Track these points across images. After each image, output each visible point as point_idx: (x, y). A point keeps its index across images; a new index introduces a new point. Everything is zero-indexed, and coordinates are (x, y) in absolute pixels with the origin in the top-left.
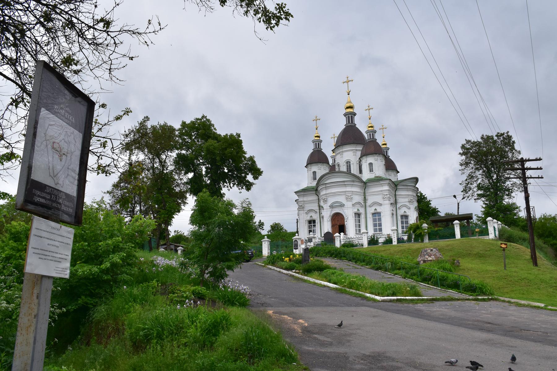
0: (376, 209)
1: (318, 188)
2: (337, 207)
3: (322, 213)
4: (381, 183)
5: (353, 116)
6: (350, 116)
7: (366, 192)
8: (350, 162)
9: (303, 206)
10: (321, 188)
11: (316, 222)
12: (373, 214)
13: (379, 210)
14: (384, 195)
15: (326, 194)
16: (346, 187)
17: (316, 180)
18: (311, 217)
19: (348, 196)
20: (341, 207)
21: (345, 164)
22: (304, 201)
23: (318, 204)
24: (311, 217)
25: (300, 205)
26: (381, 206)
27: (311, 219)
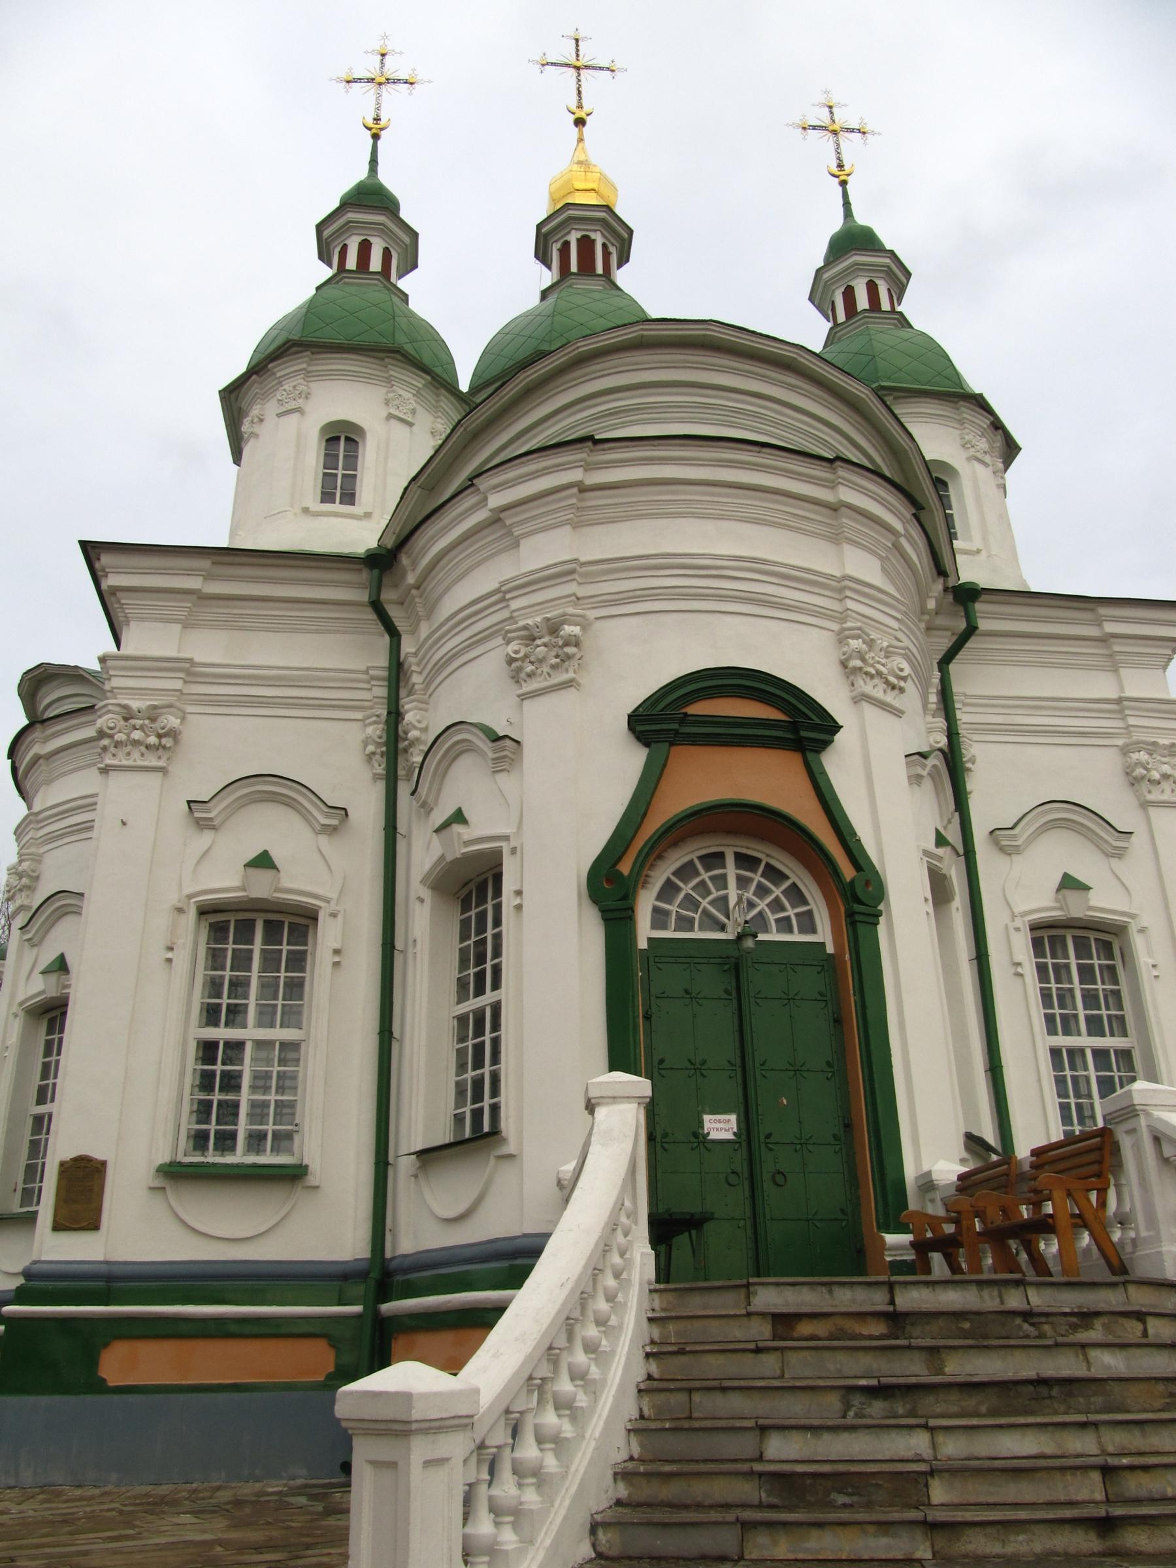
1: (430, 529)
3: (459, 817)
4: (1110, 628)
5: (613, 250)
7: (956, 688)
9: (173, 721)
10: (496, 500)
11: (328, 935)
14: (1152, 748)
15: (566, 572)
16: (836, 538)
17: (349, 498)
18: (264, 861)
19: (871, 643)
22: (189, 670)
23: (376, 731)
24: (264, 861)
25: (135, 704)
26: (1119, 854)
27: (261, 887)
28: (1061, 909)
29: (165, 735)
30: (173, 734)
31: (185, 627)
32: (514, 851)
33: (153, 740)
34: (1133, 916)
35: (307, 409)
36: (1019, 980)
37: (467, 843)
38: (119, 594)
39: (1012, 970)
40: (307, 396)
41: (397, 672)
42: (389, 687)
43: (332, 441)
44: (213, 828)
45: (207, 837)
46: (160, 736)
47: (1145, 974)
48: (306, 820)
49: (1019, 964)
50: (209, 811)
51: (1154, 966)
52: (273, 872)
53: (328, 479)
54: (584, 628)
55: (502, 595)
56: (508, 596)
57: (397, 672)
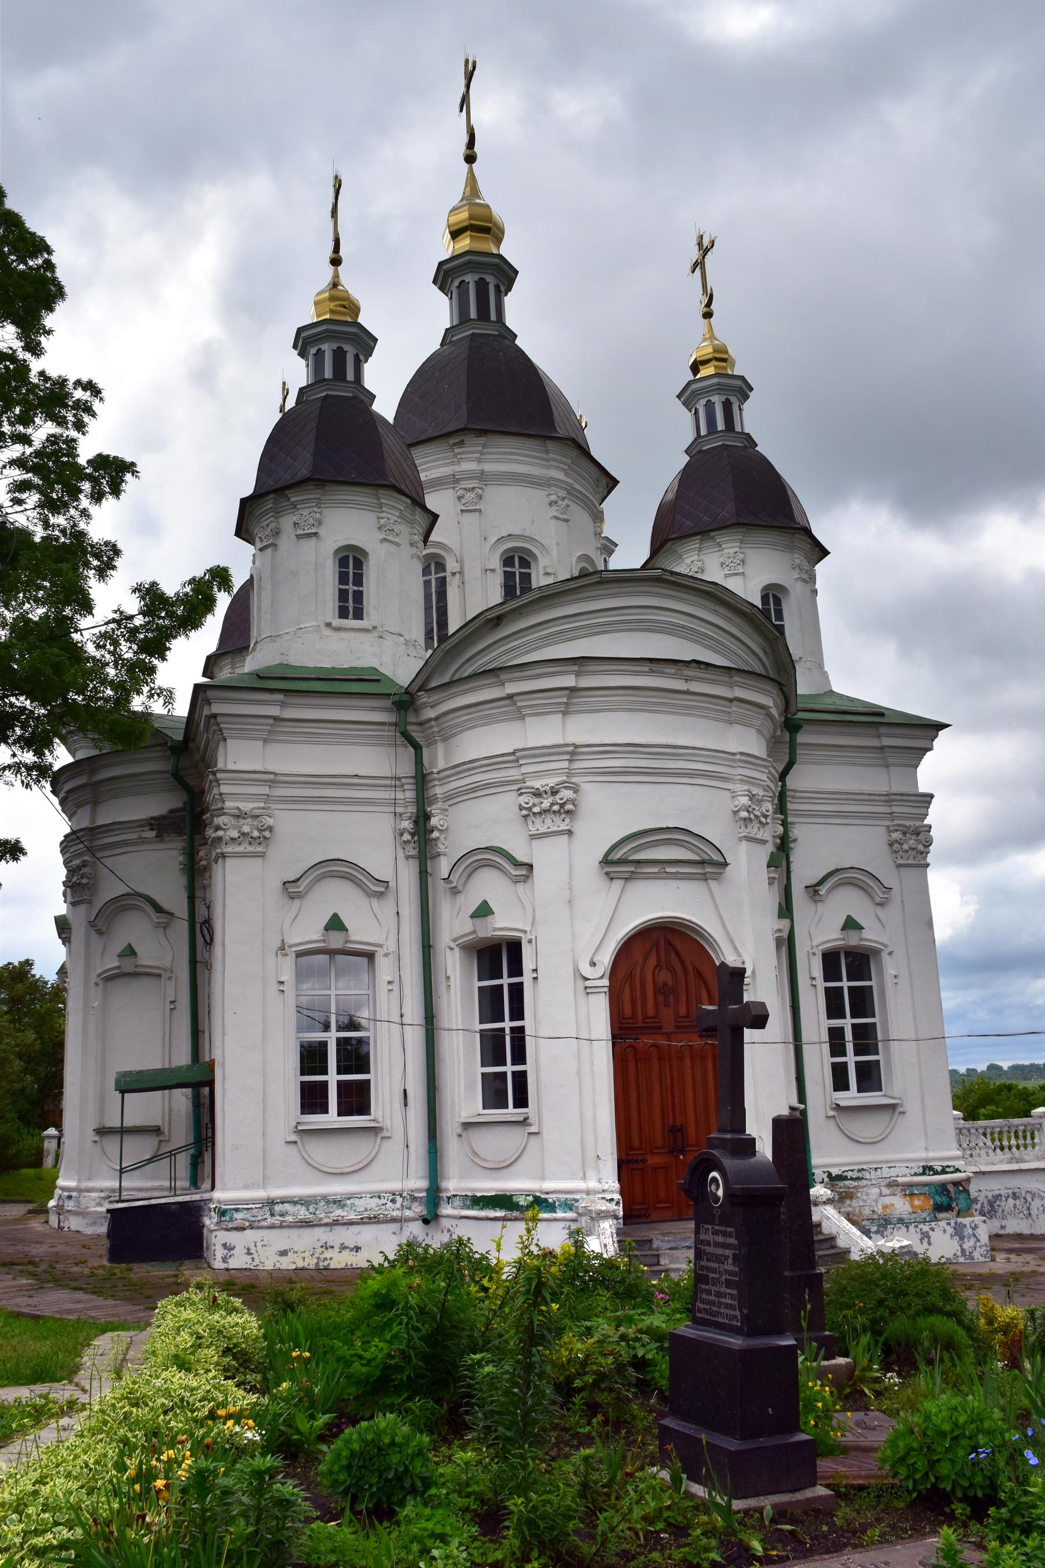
0: (851, 924)
2: (664, 869)
4: (886, 741)
6: (470, 278)
8: (525, 563)
9: (270, 821)
12: (830, 961)
13: (871, 935)
17: (359, 615)
20: (705, 878)
21: (496, 563)
22: (273, 779)
24: (335, 924)
28: (843, 939)
29: (264, 830)
30: (270, 829)
31: (265, 741)
32: (530, 941)
33: (256, 834)
34: (886, 946)
35: (322, 532)
36: (813, 989)
37: (495, 929)
38: (219, 719)
39: (809, 981)
40: (320, 523)
41: (422, 780)
42: (417, 790)
43: (343, 562)
44: (300, 897)
45: (297, 903)
46: (260, 831)
47: (889, 982)
48: (363, 890)
49: (814, 978)
50: (298, 887)
51: (895, 976)
52: (343, 933)
53: (343, 595)
54: (576, 791)
55: (515, 757)
56: (521, 762)
57: (422, 780)
